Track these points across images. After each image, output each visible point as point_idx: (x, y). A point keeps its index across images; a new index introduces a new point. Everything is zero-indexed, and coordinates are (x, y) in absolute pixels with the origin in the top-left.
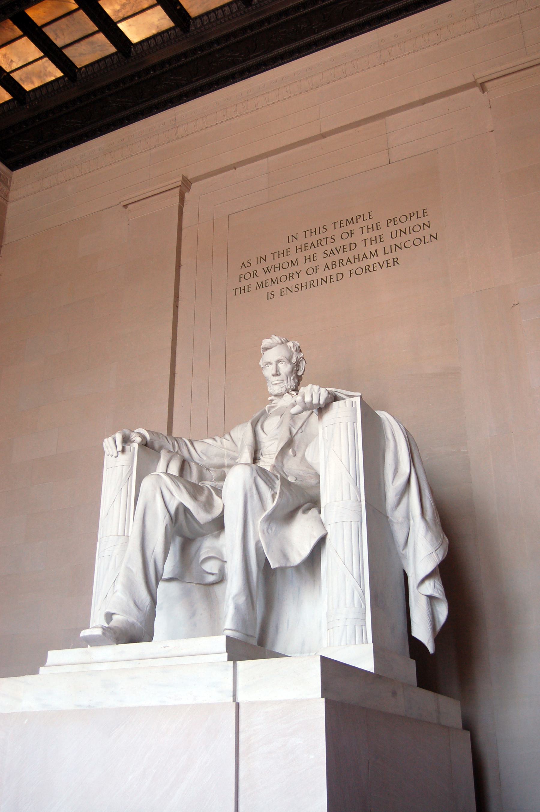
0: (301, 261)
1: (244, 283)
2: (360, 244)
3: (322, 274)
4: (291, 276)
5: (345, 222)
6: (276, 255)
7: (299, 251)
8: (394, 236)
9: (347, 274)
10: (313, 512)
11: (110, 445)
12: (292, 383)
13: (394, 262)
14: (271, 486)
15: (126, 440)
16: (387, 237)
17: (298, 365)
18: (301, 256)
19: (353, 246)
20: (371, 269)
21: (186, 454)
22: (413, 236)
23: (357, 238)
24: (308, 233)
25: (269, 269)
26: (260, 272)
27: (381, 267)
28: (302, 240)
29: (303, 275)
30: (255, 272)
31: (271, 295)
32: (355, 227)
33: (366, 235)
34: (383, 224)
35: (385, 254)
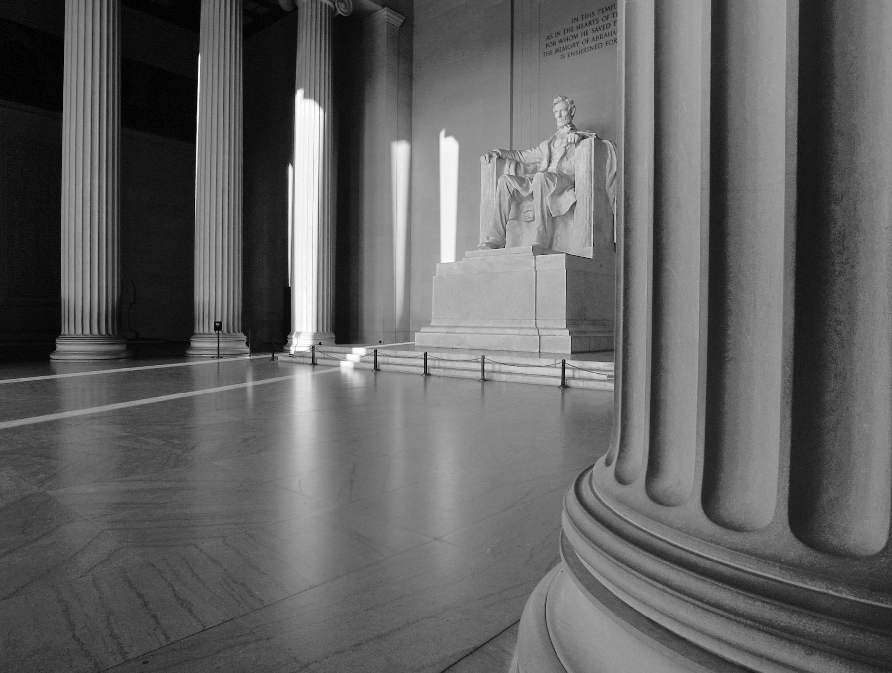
0: (580, 35)
3: (591, 44)
4: (573, 45)
9: (604, 44)
10: (572, 191)
11: (483, 160)
12: (568, 121)
14: (553, 182)
15: (490, 156)
17: (571, 110)
18: (579, 32)
21: (518, 159)
26: (558, 43)
29: (580, 43)
31: (563, 57)
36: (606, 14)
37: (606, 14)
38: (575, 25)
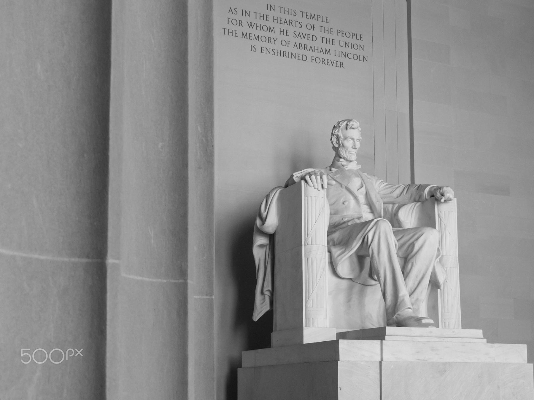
0: (277, 31)
1: (231, 27)
2: (319, 40)
4: (269, 40)
6: (258, 15)
7: (275, 21)
8: (341, 45)
9: (309, 59)
16: (337, 43)
18: (277, 26)
19: (314, 39)
20: (326, 62)
22: (353, 51)
23: (317, 32)
26: (245, 23)
28: (277, 13)
30: (241, 22)
31: (253, 48)
34: (335, 31)
37: (312, 22)
38: (271, 14)
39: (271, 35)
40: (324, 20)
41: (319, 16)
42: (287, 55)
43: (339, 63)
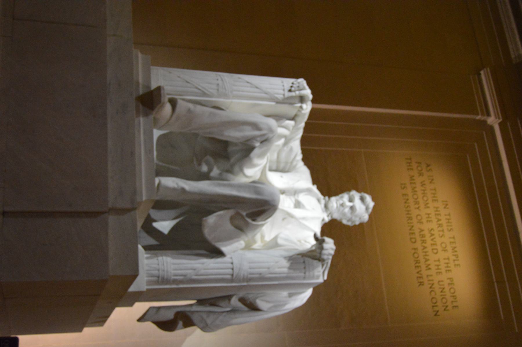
0: (428, 211)
1: (414, 165)
2: (436, 257)
4: (417, 203)
5: (454, 245)
8: (441, 283)
13: (421, 282)
18: (431, 211)
19: (435, 251)
20: (417, 265)
23: (442, 255)
24: (448, 217)
25: (424, 186)
27: (418, 272)
32: (449, 254)
33: (442, 262)
34: (449, 275)
35: (428, 276)
36: (449, 248)
37: (449, 248)
39: (422, 205)
40: (457, 263)
41: (457, 256)
42: (409, 221)
43: (421, 280)
